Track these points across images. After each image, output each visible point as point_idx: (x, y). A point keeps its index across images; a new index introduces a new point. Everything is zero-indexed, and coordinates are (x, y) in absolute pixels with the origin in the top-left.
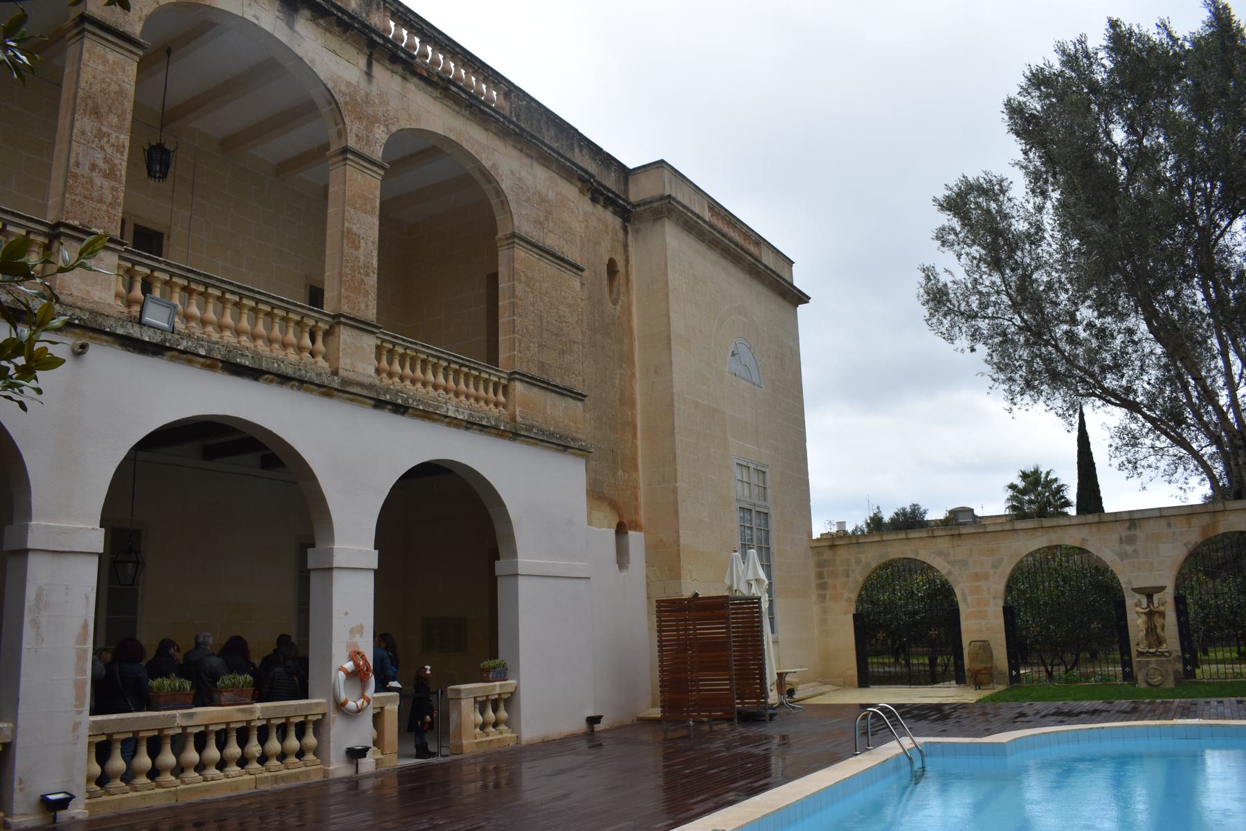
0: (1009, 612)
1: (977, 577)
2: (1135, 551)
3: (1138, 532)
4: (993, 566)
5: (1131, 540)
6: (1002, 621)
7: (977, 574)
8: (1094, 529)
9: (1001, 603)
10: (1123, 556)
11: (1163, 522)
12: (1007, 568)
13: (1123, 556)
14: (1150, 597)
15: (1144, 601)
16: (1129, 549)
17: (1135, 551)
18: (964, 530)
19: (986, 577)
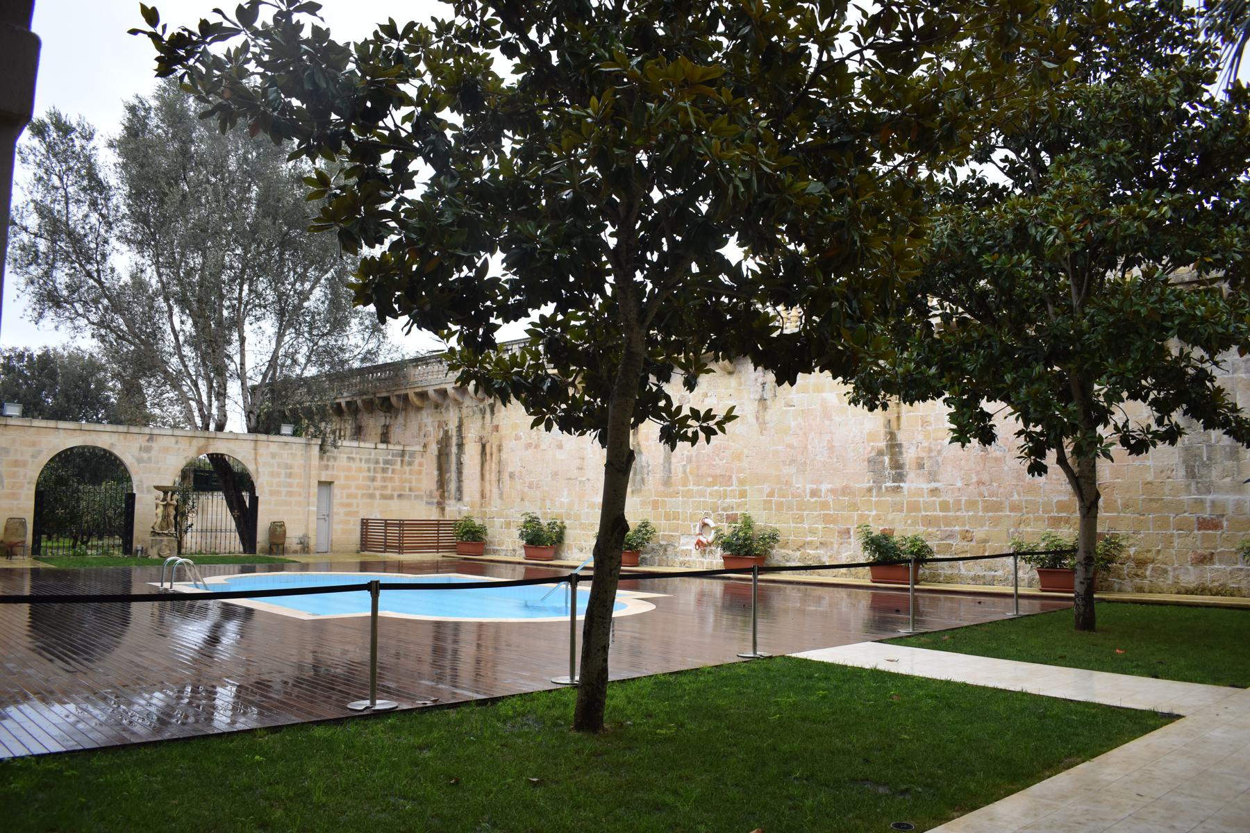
0: (39, 495)
1: (16, 463)
2: (149, 458)
3: (154, 445)
4: (33, 456)
5: (148, 450)
6: (32, 503)
7: (16, 461)
8: (122, 436)
9: (33, 487)
10: (139, 460)
11: (173, 440)
12: (45, 459)
13: (139, 460)
14: (166, 493)
15: (161, 494)
16: (145, 456)
17: (149, 458)
18: (10, 421)
19: (25, 464)
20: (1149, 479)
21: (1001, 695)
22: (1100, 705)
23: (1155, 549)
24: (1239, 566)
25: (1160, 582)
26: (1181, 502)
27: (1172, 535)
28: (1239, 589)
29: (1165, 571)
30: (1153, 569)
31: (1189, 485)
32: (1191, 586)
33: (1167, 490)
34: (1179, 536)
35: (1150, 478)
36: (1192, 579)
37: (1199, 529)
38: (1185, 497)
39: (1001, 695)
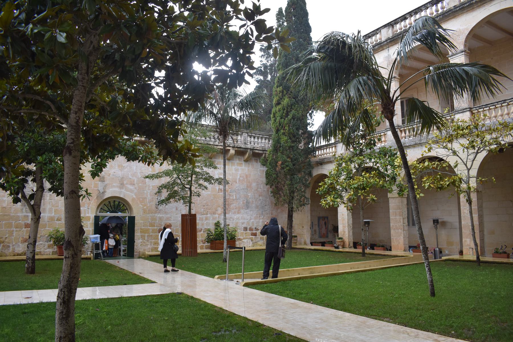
20: (4, 206)
21: (115, 300)
22: (158, 295)
23: (4, 237)
24: (41, 243)
25: (6, 252)
26: (18, 216)
27: (13, 231)
28: (40, 252)
29: (9, 247)
30: (3, 246)
31: (23, 209)
32: (20, 252)
33: (12, 210)
34: (16, 231)
35: (5, 205)
36: (20, 249)
37: (25, 228)
38: (20, 214)
39: (115, 300)
